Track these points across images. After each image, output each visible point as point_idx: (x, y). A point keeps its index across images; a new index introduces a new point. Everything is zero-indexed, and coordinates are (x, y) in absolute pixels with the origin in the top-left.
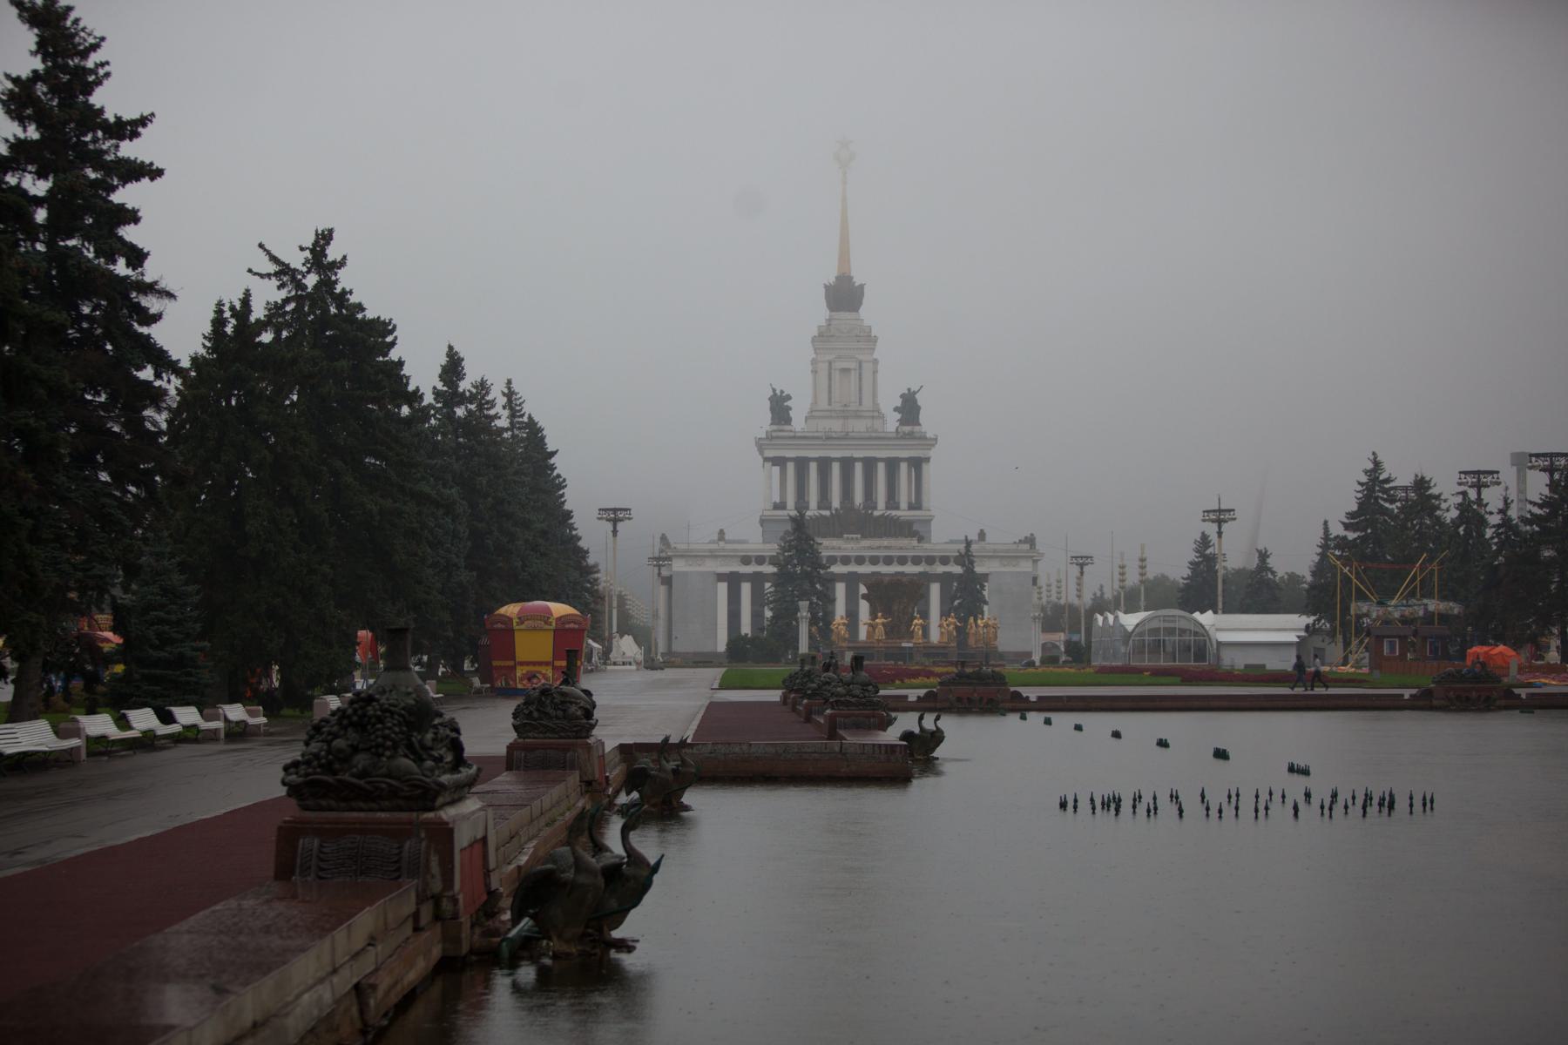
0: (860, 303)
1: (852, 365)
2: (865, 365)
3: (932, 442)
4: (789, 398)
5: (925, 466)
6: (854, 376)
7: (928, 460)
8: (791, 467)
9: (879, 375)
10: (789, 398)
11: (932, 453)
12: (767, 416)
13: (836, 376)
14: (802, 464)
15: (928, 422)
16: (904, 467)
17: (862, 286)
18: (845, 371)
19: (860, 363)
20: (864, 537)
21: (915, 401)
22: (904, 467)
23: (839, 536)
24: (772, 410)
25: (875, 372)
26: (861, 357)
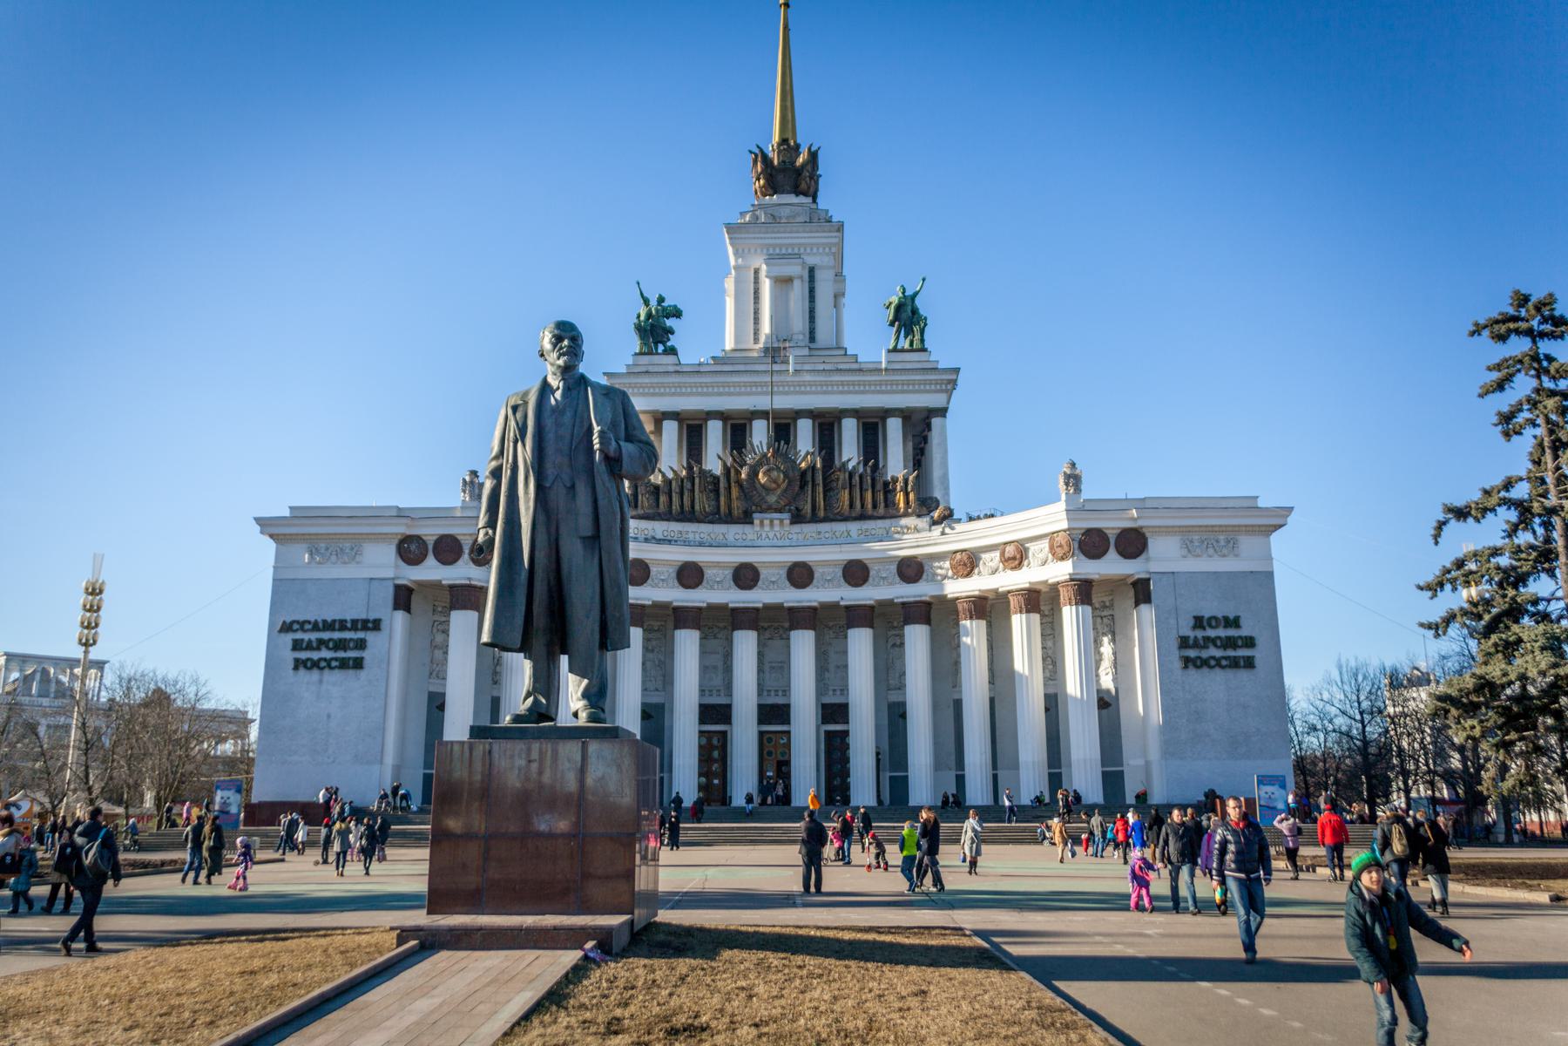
0: (814, 178)
1: (794, 269)
2: (819, 275)
3: (949, 380)
4: (677, 314)
5: (936, 422)
6: (798, 291)
7: (942, 412)
9: (846, 300)
10: (677, 314)
15: (942, 348)
16: (894, 426)
17: (813, 156)
19: (812, 270)
20: (797, 518)
21: (915, 311)
22: (894, 426)
23: (746, 518)
24: (640, 329)
25: (838, 296)
26: (811, 260)
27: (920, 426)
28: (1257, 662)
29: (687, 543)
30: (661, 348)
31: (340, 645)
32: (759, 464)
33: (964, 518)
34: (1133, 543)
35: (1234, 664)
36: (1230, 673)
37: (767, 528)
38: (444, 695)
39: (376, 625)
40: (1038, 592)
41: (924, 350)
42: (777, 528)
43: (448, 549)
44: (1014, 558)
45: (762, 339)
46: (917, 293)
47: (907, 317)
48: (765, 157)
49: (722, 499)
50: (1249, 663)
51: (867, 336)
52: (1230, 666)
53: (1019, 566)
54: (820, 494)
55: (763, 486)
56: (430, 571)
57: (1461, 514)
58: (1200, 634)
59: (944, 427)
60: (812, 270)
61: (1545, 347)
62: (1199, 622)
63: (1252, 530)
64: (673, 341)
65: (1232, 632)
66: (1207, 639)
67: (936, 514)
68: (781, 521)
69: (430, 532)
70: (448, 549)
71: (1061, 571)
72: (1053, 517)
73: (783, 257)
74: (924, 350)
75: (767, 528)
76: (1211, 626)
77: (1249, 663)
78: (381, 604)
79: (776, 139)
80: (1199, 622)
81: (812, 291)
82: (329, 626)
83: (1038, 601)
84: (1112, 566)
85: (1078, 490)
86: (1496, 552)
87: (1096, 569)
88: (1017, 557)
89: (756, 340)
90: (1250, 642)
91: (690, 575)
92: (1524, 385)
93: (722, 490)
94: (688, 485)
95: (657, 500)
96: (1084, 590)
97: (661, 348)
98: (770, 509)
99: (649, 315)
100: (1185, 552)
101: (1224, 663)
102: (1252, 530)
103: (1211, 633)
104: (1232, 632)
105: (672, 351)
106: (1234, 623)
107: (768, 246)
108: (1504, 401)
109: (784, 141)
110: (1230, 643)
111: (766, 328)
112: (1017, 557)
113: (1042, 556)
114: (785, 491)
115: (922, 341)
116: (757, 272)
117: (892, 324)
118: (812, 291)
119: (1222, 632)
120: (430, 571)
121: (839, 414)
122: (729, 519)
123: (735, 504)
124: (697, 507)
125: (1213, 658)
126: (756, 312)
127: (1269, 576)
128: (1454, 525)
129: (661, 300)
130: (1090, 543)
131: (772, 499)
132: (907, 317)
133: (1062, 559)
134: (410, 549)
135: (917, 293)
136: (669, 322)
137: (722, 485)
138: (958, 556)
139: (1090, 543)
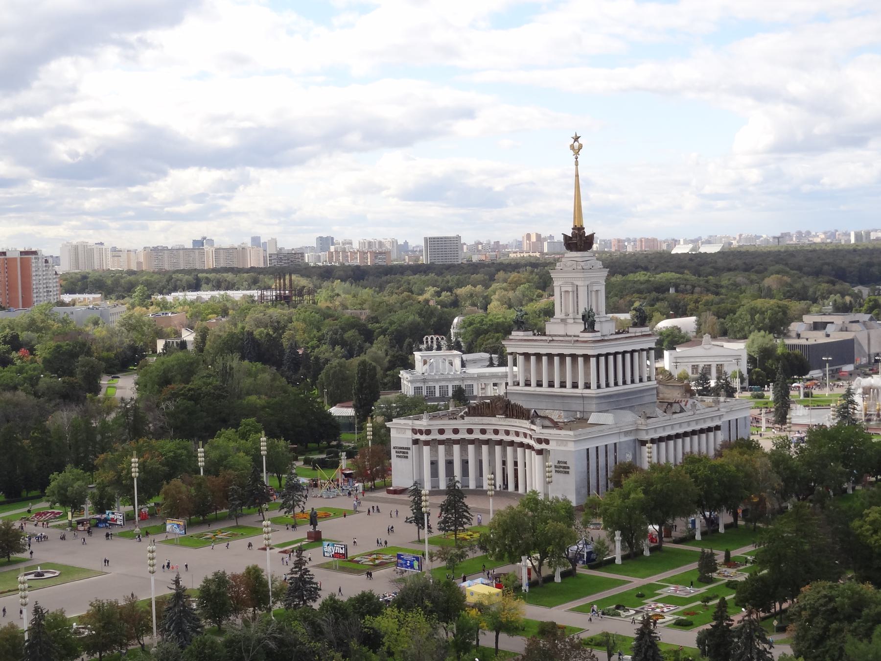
1: (570, 289)
20: (507, 416)
26: (576, 283)
31: (404, 453)
34: (547, 442)
39: (409, 449)
43: (421, 432)
50: (568, 473)
56: (418, 436)
62: (559, 462)
69: (417, 428)
70: (421, 432)
77: (568, 473)
78: (410, 445)
80: (559, 462)
82: (401, 448)
84: (543, 446)
90: (568, 468)
106: (566, 463)
110: (564, 468)
120: (418, 436)
131: (501, 412)
134: (415, 431)
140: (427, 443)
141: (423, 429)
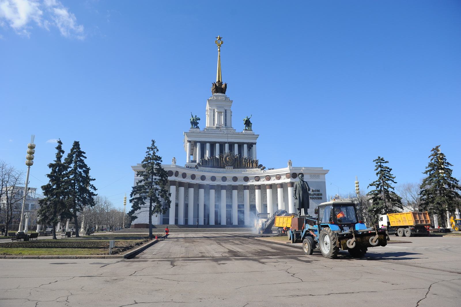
5: (254, 145)
7: (255, 144)
8: (198, 145)
10: (199, 119)
11: (257, 141)
12: (190, 126)
13: (216, 114)
14: (203, 145)
16: (245, 146)
17: (226, 85)
18: (221, 112)
19: (226, 110)
21: (249, 122)
22: (245, 146)
24: (191, 122)
26: (226, 108)
27: (250, 146)
28: (322, 198)
29: (212, 172)
30: (196, 126)
32: (227, 156)
33: (268, 169)
35: (319, 198)
36: (318, 200)
37: (228, 169)
38: (188, 204)
40: (283, 184)
41: (252, 130)
42: (230, 169)
44: (279, 178)
45: (215, 125)
46: (250, 118)
47: (248, 123)
48: (216, 85)
49: (219, 163)
50: (321, 198)
51: (239, 127)
52: (318, 199)
53: (279, 179)
54: (238, 163)
55: (228, 161)
57: (371, 185)
58: (313, 193)
59: (256, 146)
60: (226, 110)
61: (382, 164)
63: (322, 174)
64: (198, 125)
65: (318, 193)
66: (314, 194)
67: (262, 168)
68: (231, 168)
71: (288, 180)
72: (287, 170)
73: (220, 107)
74: (252, 130)
75: (228, 169)
76: (315, 192)
77: (321, 198)
79: (217, 80)
81: (226, 115)
83: (282, 186)
85: (291, 165)
86: (375, 191)
87: (293, 180)
88: (279, 177)
89: (214, 125)
90: (321, 195)
91: (213, 179)
92: (380, 169)
93: (219, 162)
94: (212, 160)
95: (207, 163)
96: (292, 184)
97: (196, 126)
98: (229, 166)
99: (193, 120)
100: (310, 178)
101: (317, 198)
102: (322, 174)
103: (315, 193)
104: (318, 193)
105: (198, 127)
106: (319, 191)
107: (217, 105)
108: (377, 171)
109: (219, 81)
110: (318, 195)
111: (216, 122)
112: (279, 177)
113: (284, 177)
114: (232, 162)
115: (251, 128)
116: (214, 110)
117: (245, 124)
118: (226, 115)
119: (317, 193)
121: (234, 143)
122: (221, 168)
123: (222, 164)
124: (214, 165)
125: (315, 197)
126: (214, 119)
127: (325, 182)
128: (370, 186)
129: (196, 116)
130: (294, 175)
132: (248, 123)
133: (288, 178)
135: (250, 118)
136: (198, 121)
137: (219, 160)
138: (267, 177)
139: (294, 175)
140: (173, 183)
141: (174, 170)
